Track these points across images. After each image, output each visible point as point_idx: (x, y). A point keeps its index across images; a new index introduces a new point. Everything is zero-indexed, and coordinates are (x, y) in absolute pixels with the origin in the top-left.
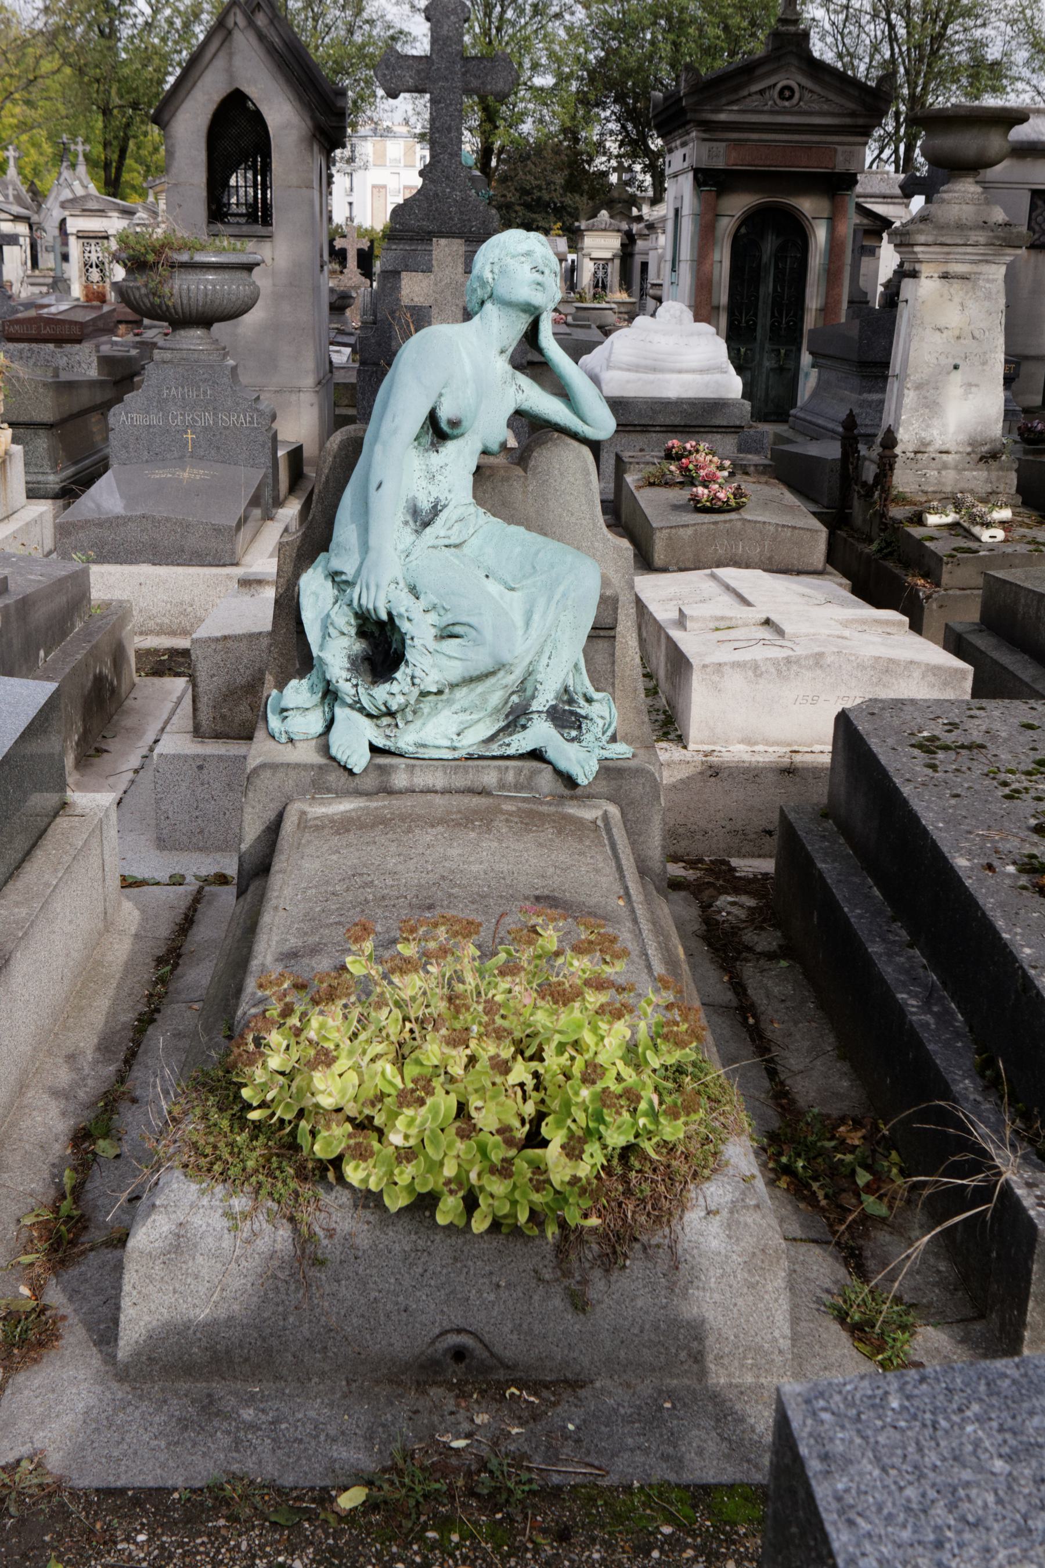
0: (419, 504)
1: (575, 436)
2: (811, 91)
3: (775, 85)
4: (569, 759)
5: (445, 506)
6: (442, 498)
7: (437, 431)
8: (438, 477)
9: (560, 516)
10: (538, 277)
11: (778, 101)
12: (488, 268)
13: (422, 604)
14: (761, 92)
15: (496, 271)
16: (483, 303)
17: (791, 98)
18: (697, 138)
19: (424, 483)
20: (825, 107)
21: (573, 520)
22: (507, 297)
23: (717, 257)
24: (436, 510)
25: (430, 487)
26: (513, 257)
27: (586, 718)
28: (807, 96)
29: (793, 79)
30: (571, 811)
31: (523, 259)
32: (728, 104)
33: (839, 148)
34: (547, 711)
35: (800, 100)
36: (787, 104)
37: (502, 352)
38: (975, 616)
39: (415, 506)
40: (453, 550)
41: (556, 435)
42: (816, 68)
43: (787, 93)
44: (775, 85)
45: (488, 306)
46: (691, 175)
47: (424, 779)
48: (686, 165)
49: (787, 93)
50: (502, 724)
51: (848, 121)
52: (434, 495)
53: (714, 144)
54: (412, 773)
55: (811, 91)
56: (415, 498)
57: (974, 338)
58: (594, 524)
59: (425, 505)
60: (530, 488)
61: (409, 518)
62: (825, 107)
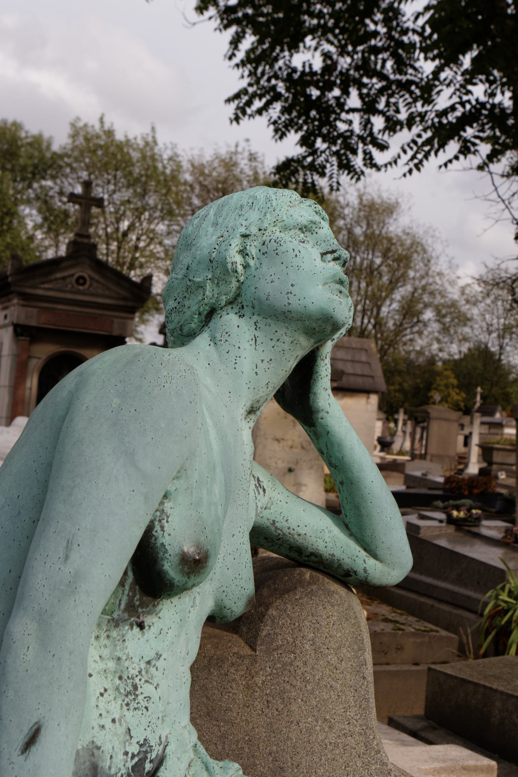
1: (345, 576)
2: (98, 282)
3: (73, 275)
7: (149, 577)
8: (146, 689)
9: (310, 731)
11: (75, 285)
12: (236, 243)
14: (64, 278)
15: (253, 251)
16: (210, 314)
17: (83, 284)
18: (18, 304)
19: (115, 708)
20: (107, 293)
21: (332, 737)
22: (280, 301)
23: (28, 384)
25: (132, 718)
26: (286, 228)
28: (95, 284)
29: (87, 273)
32: (43, 283)
33: (116, 320)
35: (90, 286)
36: (81, 288)
38: (419, 710)
41: (308, 574)
42: (101, 267)
43: (81, 281)
44: (73, 275)
45: (230, 320)
46: (10, 329)
48: (7, 321)
49: (81, 281)
51: (121, 303)
52: (139, 735)
53: (30, 309)
55: (98, 282)
56: (94, 749)
57: (303, 448)
60: (259, 680)
62: (107, 293)
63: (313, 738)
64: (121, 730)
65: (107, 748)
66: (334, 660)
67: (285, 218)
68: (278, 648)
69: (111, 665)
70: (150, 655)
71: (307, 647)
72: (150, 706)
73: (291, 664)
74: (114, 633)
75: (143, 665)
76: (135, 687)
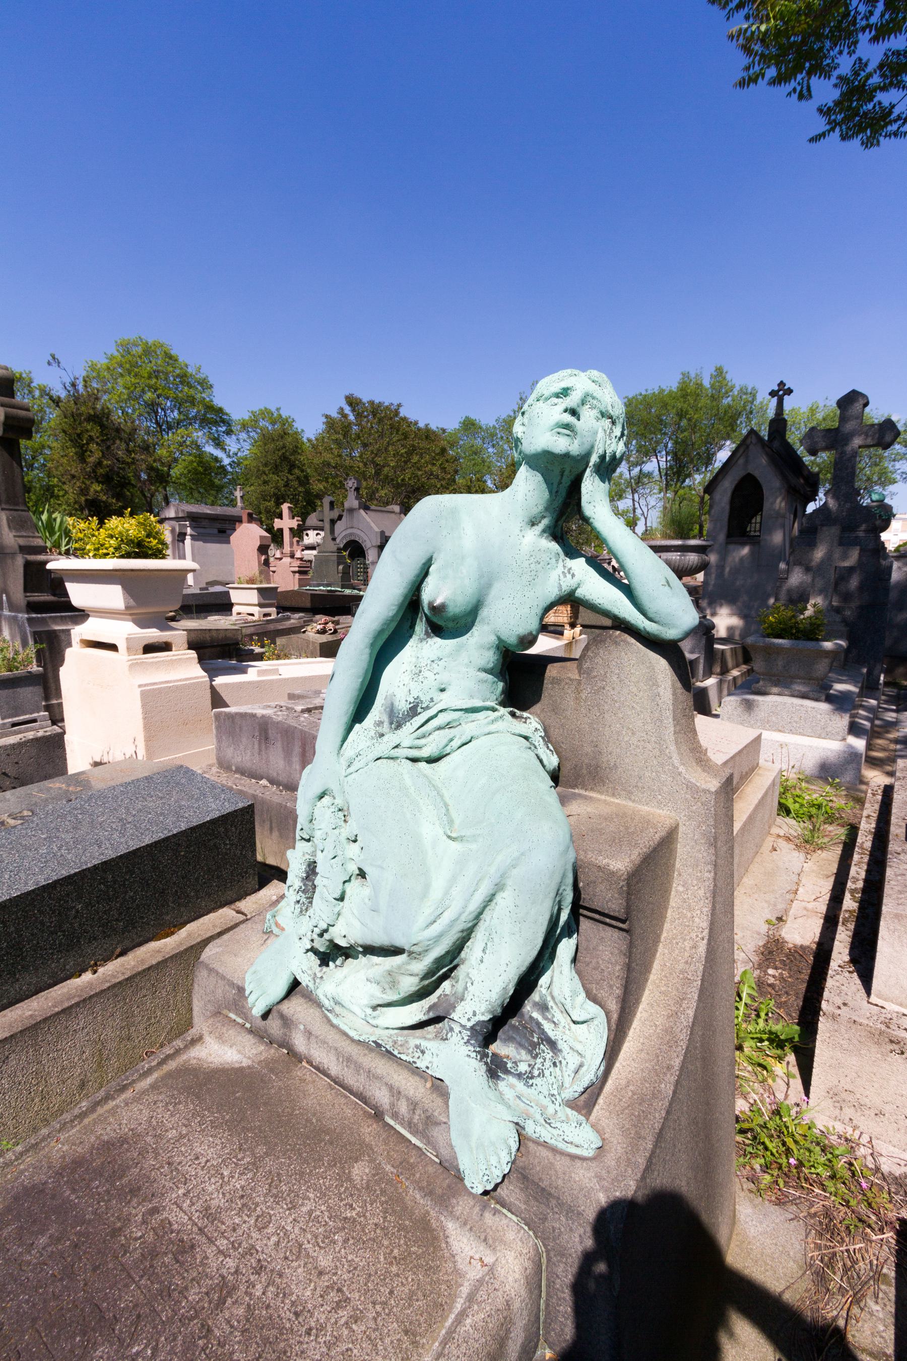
0: (396, 704)
4: (466, 1135)
5: (427, 708)
6: (425, 699)
9: (618, 733)
10: (568, 418)
13: (347, 831)
19: (406, 678)
24: (413, 711)
27: (552, 1044)
30: (451, 1226)
31: (555, 400)
34: (472, 1028)
37: (533, 524)
39: (392, 704)
40: (423, 765)
47: (319, 1055)
50: (425, 1018)
54: (309, 1039)
58: (661, 751)
59: (403, 706)
61: (385, 718)
63: (621, 738)
64: (406, 690)
65: (398, 696)
66: (635, 690)
67: (544, 392)
68: (595, 677)
69: (414, 660)
70: (434, 658)
71: (615, 678)
72: (425, 682)
73: (604, 688)
74: (419, 645)
75: (429, 662)
76: (420, 672)
